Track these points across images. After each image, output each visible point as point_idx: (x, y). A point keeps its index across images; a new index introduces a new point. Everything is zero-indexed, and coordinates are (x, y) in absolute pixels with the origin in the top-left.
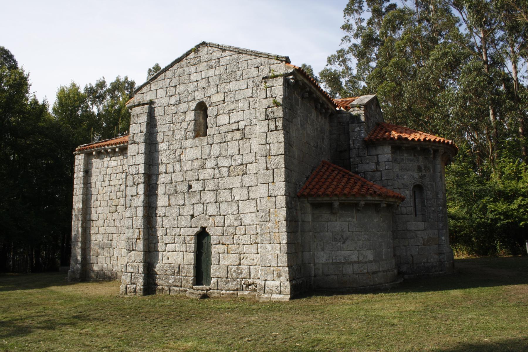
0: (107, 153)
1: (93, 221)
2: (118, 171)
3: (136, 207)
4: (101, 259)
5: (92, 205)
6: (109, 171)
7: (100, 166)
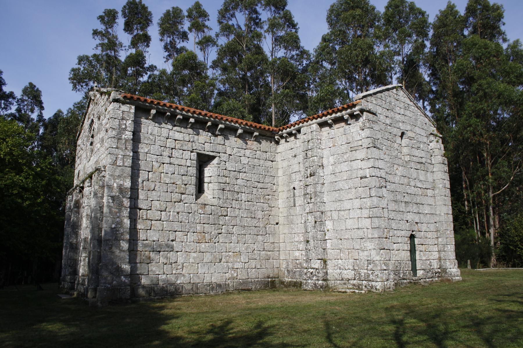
0: (172, 119)
1: (140, 209)
2: (185, 148)
3: (383, 208)
4: (153, 267)
5: (140, 185)
6: (170, 143)
7: (155, 132)
